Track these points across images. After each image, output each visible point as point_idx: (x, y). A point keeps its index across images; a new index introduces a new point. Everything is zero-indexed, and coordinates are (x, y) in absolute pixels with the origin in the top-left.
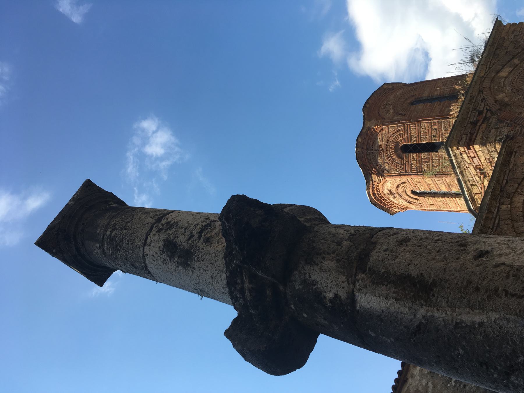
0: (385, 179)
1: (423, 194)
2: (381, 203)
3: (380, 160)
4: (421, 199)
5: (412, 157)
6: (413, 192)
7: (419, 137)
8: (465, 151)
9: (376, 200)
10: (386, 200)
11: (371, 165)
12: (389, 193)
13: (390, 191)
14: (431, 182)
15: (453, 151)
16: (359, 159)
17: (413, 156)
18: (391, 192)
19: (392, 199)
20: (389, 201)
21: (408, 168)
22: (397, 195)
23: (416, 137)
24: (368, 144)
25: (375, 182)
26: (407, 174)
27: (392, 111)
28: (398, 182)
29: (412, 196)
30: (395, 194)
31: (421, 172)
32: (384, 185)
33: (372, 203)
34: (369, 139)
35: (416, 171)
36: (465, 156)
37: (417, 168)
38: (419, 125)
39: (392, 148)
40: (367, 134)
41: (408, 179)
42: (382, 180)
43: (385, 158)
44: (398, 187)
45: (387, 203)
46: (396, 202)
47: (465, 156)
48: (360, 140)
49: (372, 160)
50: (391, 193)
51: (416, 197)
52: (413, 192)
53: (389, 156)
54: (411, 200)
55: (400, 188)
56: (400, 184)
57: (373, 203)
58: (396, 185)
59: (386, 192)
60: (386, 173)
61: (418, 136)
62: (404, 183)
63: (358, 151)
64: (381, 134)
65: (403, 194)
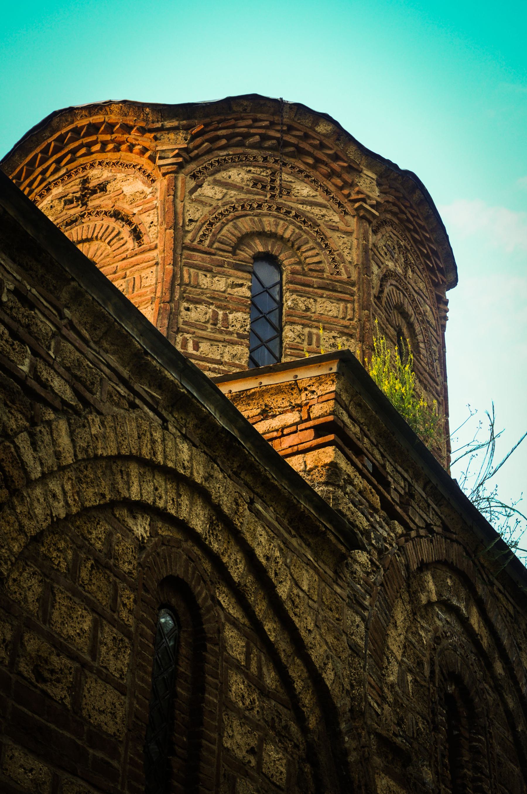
0: (164, 175)
2: (45, 151)
5: (240, 282)
8: (309, 419)
9: (63, 131)
10: (56, 170)
11: (224, 142)
12: (93, 184)
15: (319, 380)
16: (254, 98)
17: (241, 285)
18: (94, 192)
19: (56, 191)
20: (51, 179)
23: (308, 309)
24: (299, 152)
25: (156, 139)
30: (85, 204)
31: (182, 298)
32: (131, 170)
33: (55, 114)
34: (318, 161)
35: (186, 280)
36: (292, 418)
37: (197, 286)
38: (346, 331)
39: (277, 225)
40: (336, 158)
41: (154, 253)
42: (160, 162)
43: (242, 196)
44: (117, 215)
45: (43, 172)
47: (292, 418)
48: (322, 128)
49: (240, 150)
55: (112, 223)
56: (130, 223)
57: (56, 120)
58: (125, 207)
60: (184, 183)
61: (310, 319)
62: (137, 235)
63: (287, 109)
64: (325, 202)
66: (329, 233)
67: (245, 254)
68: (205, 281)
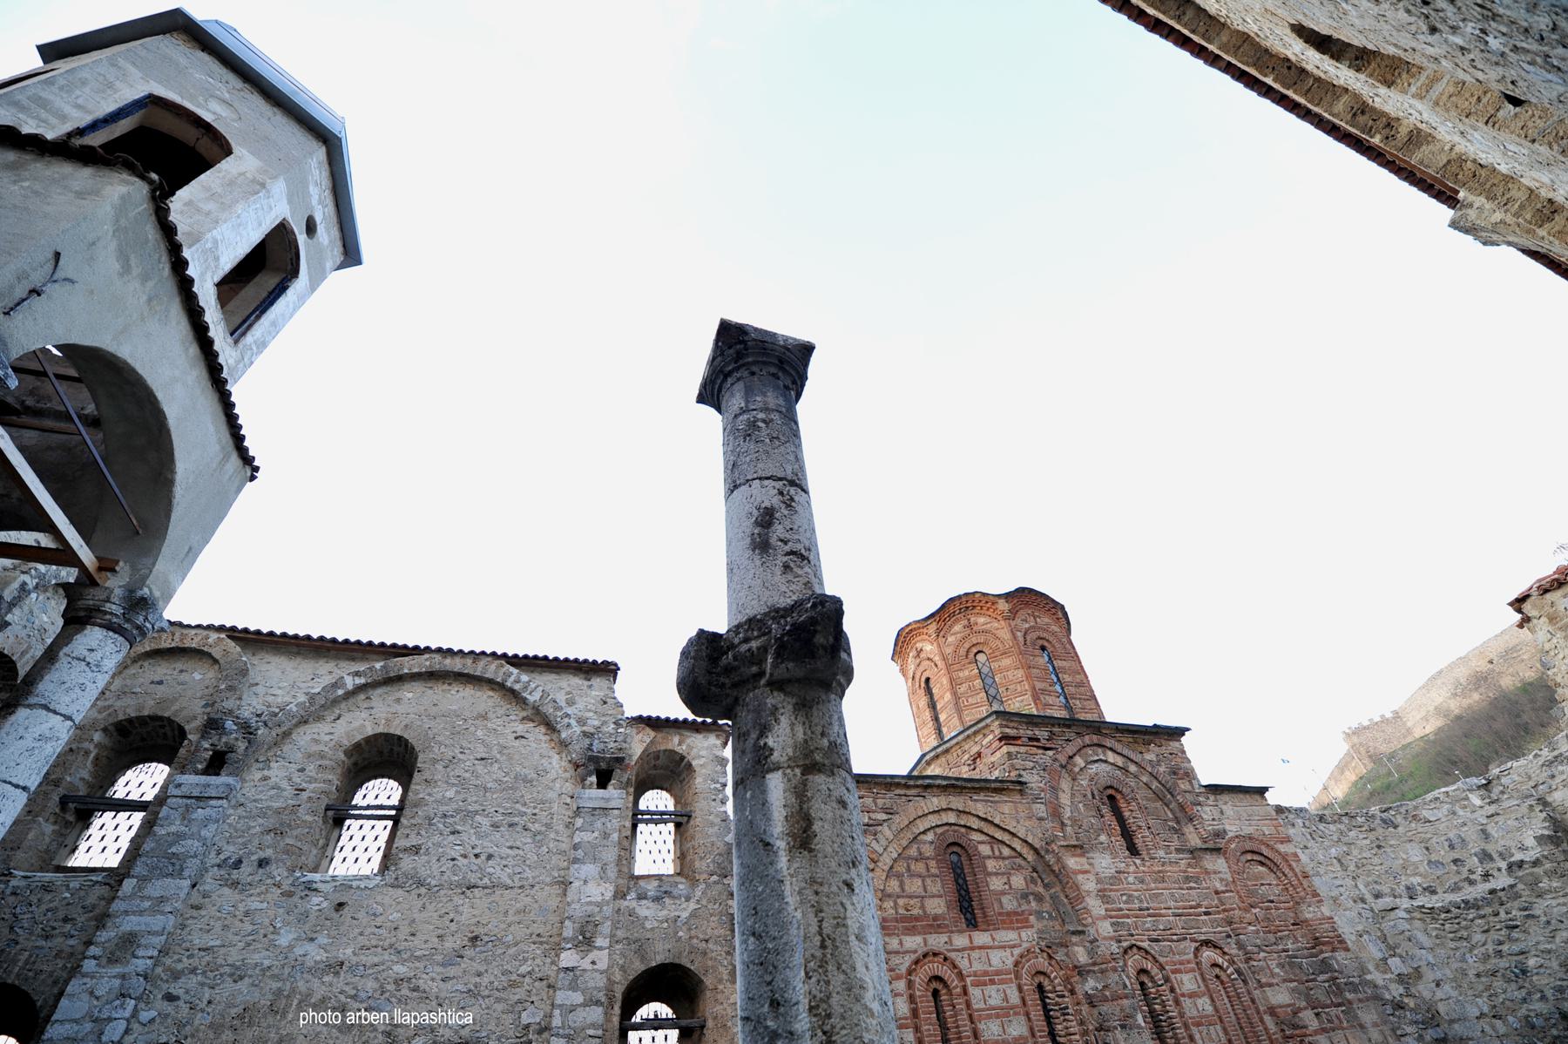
1: (929, 691)
3: (957, 628)
4: (922, 692)
6: (928, 680)
7: (1001, 671)
13: (921, 650)
14: (946, 700)
21: (956, 667)
22: (918, 661)
26: (948, 666)
27: (1027, 626)
28: (937, 659)
29: (923, 679)
44: (929, 659)
46: (910, 660)
48: (977, 595)
50: (920, 652)
51: (923, 685)
52: (928, 680)
54: (917, 680)
59: (919, 645)
65: (921, 668)
66: (995, 632)
67: (971, 655)
68: (961, 674)
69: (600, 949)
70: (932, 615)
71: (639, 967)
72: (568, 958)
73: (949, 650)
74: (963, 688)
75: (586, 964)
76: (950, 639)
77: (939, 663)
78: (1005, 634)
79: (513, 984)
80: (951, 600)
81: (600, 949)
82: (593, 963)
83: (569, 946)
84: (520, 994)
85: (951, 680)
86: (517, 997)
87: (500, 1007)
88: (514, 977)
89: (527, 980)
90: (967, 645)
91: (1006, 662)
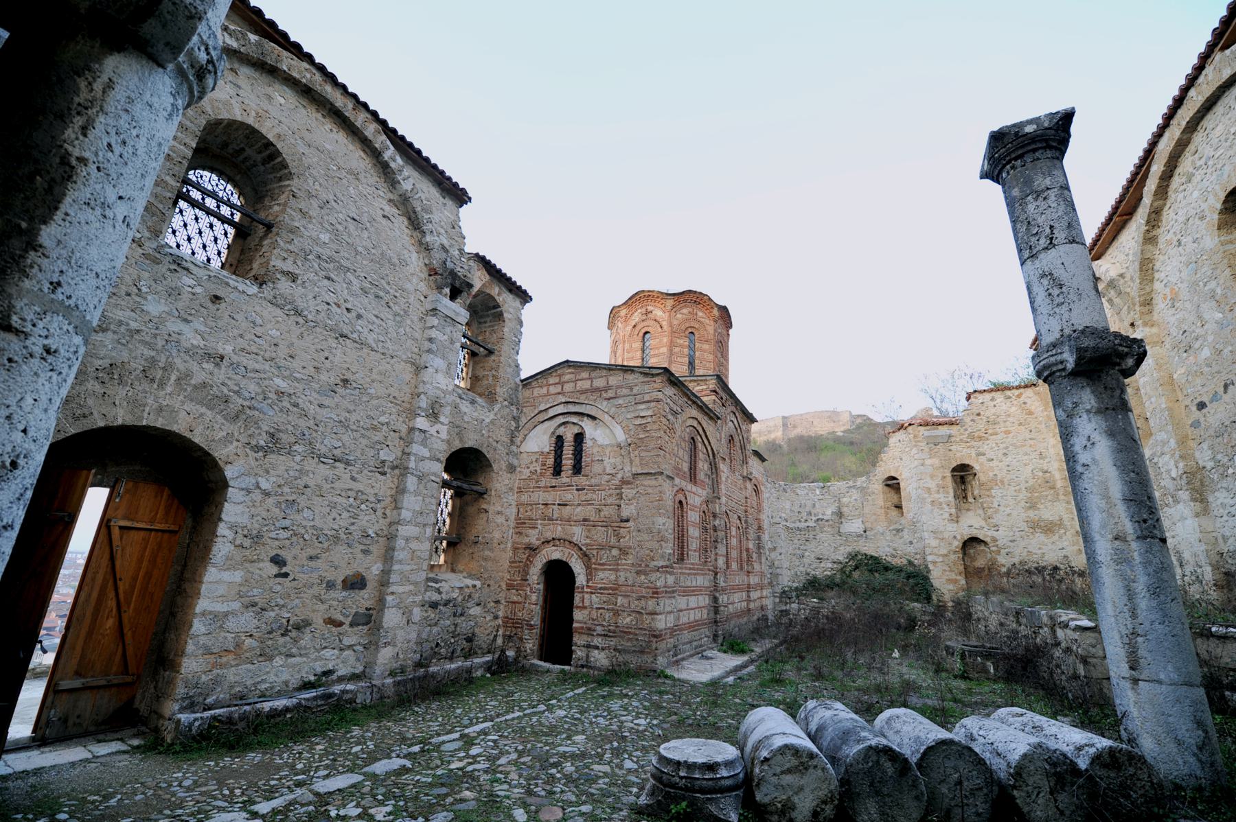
3: (685, 311)
7: (701, 350)
22: (644, 317)
26: (673, 332)
28: (664, 324)
29: (643, 331)
36: (705, 387)
47: (705, 387)
50: (647, 313)
53: (687, 320)
59: (650, 308)
65: (645, 323)
69: (442, 424)
70: (674, 295)
71: (457, 445)
72: (421, 423)
73: (676, 322)
74: (677, 350)
75: (433, 431)
76: (679, 316)
77: (665, 327)
78: (711, 329)
79: (374, 428)
80: (690, 291)
81: (442, 424)
82: (438, 432)
83: (423, 414)
84: (378, 436)
85: (671, 341)
86: (377, 438)
87: (364, 441)
88: (375, 423)
89: (385, 428)
90: (687, 325)
91: (706, 346)
